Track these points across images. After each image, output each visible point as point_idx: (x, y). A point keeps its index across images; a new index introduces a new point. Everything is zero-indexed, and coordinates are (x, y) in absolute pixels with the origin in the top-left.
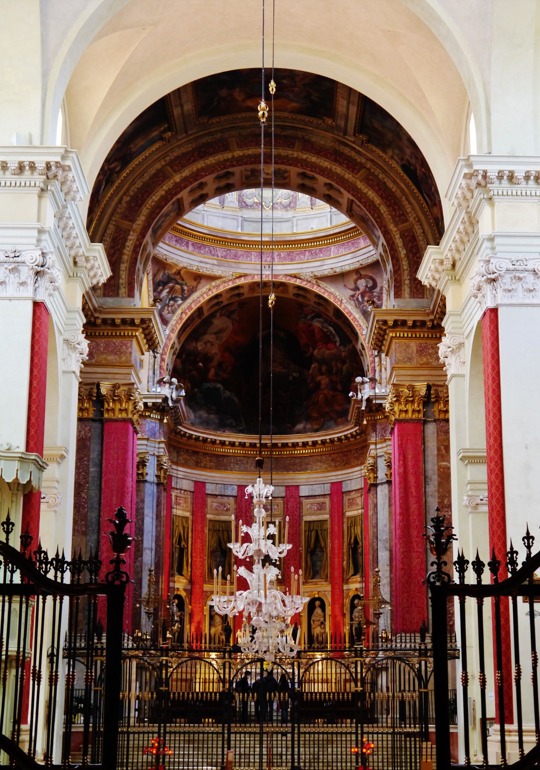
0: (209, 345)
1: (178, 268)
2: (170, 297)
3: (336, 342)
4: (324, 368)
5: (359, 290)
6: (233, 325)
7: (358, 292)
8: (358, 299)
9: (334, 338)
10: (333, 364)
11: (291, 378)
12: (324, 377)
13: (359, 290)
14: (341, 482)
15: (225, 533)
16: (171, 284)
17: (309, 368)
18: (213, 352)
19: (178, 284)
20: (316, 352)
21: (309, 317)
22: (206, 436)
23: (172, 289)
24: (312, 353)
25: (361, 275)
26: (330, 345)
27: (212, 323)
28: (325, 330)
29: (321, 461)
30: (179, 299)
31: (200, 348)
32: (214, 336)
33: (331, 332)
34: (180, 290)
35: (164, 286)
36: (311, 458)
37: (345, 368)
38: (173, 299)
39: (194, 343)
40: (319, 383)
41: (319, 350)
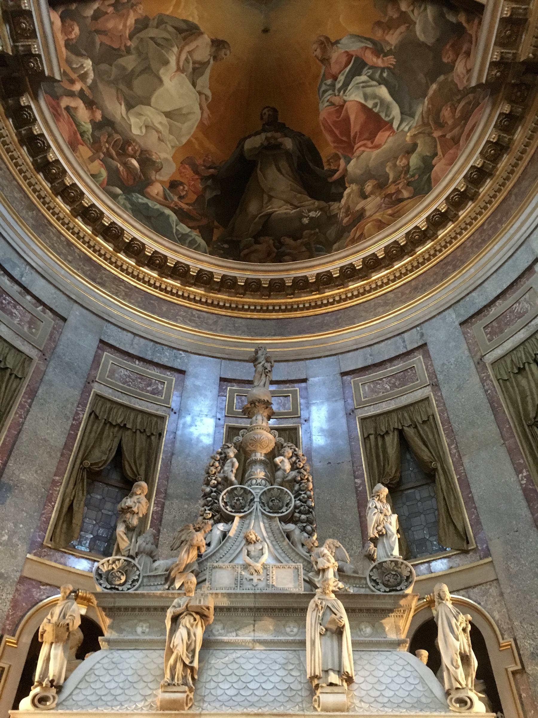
0: (154, 136)
3: (393, 118)
4: (368, 187)
6: (201, 108)
10: (387, 170)
12: (369, 199)
15: (141, 439)
17: (338, 197)
18: (163, 155)
21: (341, 78)
22: (119, 222)
24: (346, 170)
26: (382, 136)
27: (161, 81)
28: (370, 104)
31: (135, 131)
32: (165, 120)
33: (382, 101)
37: (414, 160)
39: (123, 107)
40: (363, 210)
41: (358, 157)
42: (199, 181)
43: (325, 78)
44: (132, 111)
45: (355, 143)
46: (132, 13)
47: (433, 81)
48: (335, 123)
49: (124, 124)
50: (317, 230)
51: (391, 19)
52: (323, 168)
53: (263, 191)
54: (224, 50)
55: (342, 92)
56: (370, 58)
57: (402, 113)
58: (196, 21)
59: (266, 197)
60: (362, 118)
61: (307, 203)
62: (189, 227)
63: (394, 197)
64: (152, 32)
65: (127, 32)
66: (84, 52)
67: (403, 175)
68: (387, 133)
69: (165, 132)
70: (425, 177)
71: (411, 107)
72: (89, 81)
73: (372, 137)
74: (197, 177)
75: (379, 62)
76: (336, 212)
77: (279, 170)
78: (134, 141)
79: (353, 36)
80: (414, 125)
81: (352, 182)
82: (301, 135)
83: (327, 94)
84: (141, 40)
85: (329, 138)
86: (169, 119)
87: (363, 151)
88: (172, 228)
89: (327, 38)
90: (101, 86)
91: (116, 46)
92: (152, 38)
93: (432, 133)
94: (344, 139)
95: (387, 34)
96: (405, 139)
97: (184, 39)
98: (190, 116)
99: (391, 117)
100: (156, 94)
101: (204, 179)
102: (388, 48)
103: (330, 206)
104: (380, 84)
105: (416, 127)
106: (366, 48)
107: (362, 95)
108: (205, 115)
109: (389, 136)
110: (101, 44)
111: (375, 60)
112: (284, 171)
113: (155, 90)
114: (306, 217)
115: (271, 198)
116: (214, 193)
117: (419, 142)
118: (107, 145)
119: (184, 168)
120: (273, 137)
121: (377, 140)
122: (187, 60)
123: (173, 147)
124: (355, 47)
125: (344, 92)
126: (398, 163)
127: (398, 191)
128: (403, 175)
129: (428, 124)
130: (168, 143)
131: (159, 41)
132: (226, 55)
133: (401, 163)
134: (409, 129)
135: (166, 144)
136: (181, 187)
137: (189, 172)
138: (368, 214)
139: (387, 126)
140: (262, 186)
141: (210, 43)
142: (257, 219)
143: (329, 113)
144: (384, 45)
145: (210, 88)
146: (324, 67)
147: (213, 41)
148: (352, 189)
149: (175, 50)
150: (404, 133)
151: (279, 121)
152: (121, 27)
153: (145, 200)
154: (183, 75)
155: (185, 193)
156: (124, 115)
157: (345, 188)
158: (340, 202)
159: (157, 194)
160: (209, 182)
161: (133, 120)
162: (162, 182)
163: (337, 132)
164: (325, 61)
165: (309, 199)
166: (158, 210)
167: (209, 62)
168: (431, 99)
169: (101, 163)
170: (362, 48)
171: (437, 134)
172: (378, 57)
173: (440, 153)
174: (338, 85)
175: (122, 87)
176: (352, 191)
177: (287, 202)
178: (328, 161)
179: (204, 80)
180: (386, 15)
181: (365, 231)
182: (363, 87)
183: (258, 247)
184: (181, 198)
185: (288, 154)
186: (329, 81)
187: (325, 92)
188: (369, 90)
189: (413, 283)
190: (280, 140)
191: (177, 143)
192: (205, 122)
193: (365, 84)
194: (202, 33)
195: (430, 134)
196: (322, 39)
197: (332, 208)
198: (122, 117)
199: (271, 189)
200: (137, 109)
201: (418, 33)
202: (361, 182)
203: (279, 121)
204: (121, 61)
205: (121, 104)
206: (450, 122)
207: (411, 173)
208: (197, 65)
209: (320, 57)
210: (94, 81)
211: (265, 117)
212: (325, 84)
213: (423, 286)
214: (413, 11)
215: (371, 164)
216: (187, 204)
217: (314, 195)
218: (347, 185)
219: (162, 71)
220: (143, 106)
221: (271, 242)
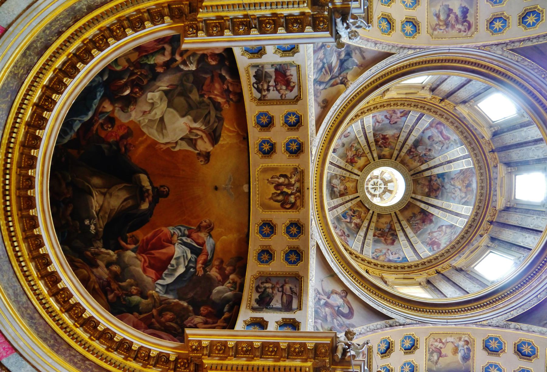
0: (147, 108)
1: (349, 83)
2: (326, 66)
3: (164, 279)
4: (115, 268)
5: (329, 298)
7: (325, 297)
8: (320, 299)
9: (167, 275)
10: (128, 280)
11: (87, 222)
12: (105, 269)
13: (329, 298)
14: (16, 350)
16: (336, 70)
17: (106, 247)
18: (133, 114)
19: (331, 79)
20: (130, 253)
21: (189, 241)
23: (331, 69)
24: (127, 249)
25: (346, 297)
26: (152, 273)
27: (183, 116)
28: (173, 262)
29: (16, 295)
30: (317, 77)
31: (150, 95)
32: (158, 117)
33: (175, 270)
34: (322, 80)
35: (341, 60)
36: (11, 274)
37: (136, 298)
38: (323, 67)
40: (97, 266)
41: (137, 258)
42: (115, 139)
43: (189, 229)
44: (163, 94)
45: (146, 254)
46: (224, 100)
47: (189, 303)
48: (160, 239)
49: (154, 87)
50: (80, 232)
51: (225, 269)
52: (128, 232)
53: (109, 188)
54: (203, 160)
55: (180, 242)
56: (202, 258)
57: (168, 285)
58: (220, 142)
59: (104, 190)
60: (164, 257)
61: (101, 222)
62: (78, 130)
63: (108, 288)
64: (213, 113)
65: (213, 96)
66: (200, 66)
67: (124, 292)
68: (154, 277)
69: (150, 116)
70: (124, 309)
71: (171, 290)
72: (182, 67)
73: (151, 266)
74: (118, 138)
75: (199, 265)
76: (96, 245)
77: (125, 200)
78: (143, 94)
79: (215, 246)
80: (160, 295)
81: (119, 255)
82: (151, 214)
83: (179, 232)
84: (208, 105)
85: (149, 235)
86: (158, 120)
87: (141, 261)
88: (77, 117)
89: (212, 229)
90: (179, 74)
91: (205, 88)
92: (209, 113)
93: (155, 309)
94: (149, 246)
95: (216, 268)
96: (150, 290)
97: (210, 134)
98: (161, 135)
99: (165, 278)
100: (175, 112)
101: (117, 143)
102: (208, 270)
103: (99, 240)
104: (186, 267)
105: (159, 296)
106: (208, 255)
107: (178, 256)
108: (162, 146)
109: (152, 278)
110: (205, 79)
111: (201, 262)
112: (124, 204)
113: (177, 111)
114: (90, 222)
115: (104, 194)
116: (106, 151)
117: (149, 300)
118: (139, 73)
119: (125, 129)
120: (149, 194)
121: (150, 270)
122: (197, 135)
123: (139, 121)
124: (208, 247)
125: (180, 243)
126: (134, 287)
127: (112, 291)
128: (124, 292)
129: (161, 305)
130: (142, 118)
131: (208, 118)
132: (201, 161)
133: (134, 289)
134: (157, 292)
135: (141, 117)
136: (110, 126)
137: (121, 133)
138: (95, 270)
139: (159, 276)
140: (114, 187)
141: (208, 151)
142: (87, 184)
143: (166, 234)
144: (210, 267)
145: (180, 150)
146: (195, 228)
147: (209, 153)
148: (114, 256)
149: (203, 128)
150: (154, 289)
151: (160, 199)
152: (216, 92)
153: (99, 98)
154: (187, 132)
155: (106, 128)
156: (160, 88)
157: (113, 251)
158: (103, 248)
159: (104, 107)
160: (115, 147)
161: (157, 94)
162: (113, 111)
163: (154, 241)
164: (200, 229)
165: (105, 224)
166: (91, 106)
167: (196, 149)
168: (177, 304)
169: (126, 67)
170: (207, 252)
171: (154, 312)
172: (202, 264)
173: (142, 316)
174: (184, 239)
175: (179, 89)
176: (111, 256)
177: (101, 207)
178: (133, 236)
179: (184, 146)
180: (227, 266)
181: (81, 270)
182: (184, 256)
183: (64, 186)
184: (102, 125)
185: (138, 205)
186: (186, 232)
187: (180, 230)
188: (182, 260)
189: (36, 315)
190: (147, 200)
191: (142, 125)
192: (157, 146)
193: (186, 257)
194: (213, 146)
195: (154, 307)
196: (212, 225)
197: (98, 242)
198: (159, 87)
199: (111, 195)
200: (165, 98)
201: (217, 288)
202: (119, 261)
203: (160, 199)
204: (195, 91)
205: (167, 87)
206: (163, 319)
207: (126, 298)
208: (194, 141)
209: (201, 225)
210: (182, 70)
211: (162, 189)
212: (185, 230)
213: (35, 323)
214: (230, 283)
215: (133, 268)
216: (97, 129)
217: (107, 227)
218: (116, 252)
219: (190, 117)
220: (167, 102)
221: (68, 196)
